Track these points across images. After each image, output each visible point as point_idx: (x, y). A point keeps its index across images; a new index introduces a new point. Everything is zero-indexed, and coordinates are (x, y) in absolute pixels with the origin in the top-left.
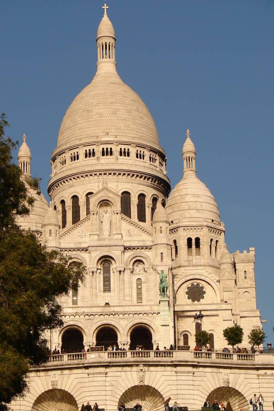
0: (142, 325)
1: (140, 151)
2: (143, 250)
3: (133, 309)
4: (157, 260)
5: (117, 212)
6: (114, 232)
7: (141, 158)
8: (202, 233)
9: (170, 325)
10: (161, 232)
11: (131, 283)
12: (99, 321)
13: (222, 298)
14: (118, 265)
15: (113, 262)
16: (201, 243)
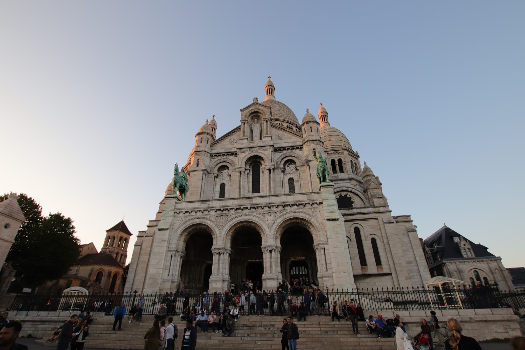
0: (297, 221)
1: (290, 126)
2: (294, 151)
3: (284, 199)
4: (309, 156)
5: (266, 119)
6: (264, 136)
7: (290, 128)
8: (342, 155)
9: (340, 219)
10: (312, 132)
11: (283, 182)
12: (235, 218)
13: (371, 205)
14: (267, 164)
15: (262, 162)
16: (343, 163)
